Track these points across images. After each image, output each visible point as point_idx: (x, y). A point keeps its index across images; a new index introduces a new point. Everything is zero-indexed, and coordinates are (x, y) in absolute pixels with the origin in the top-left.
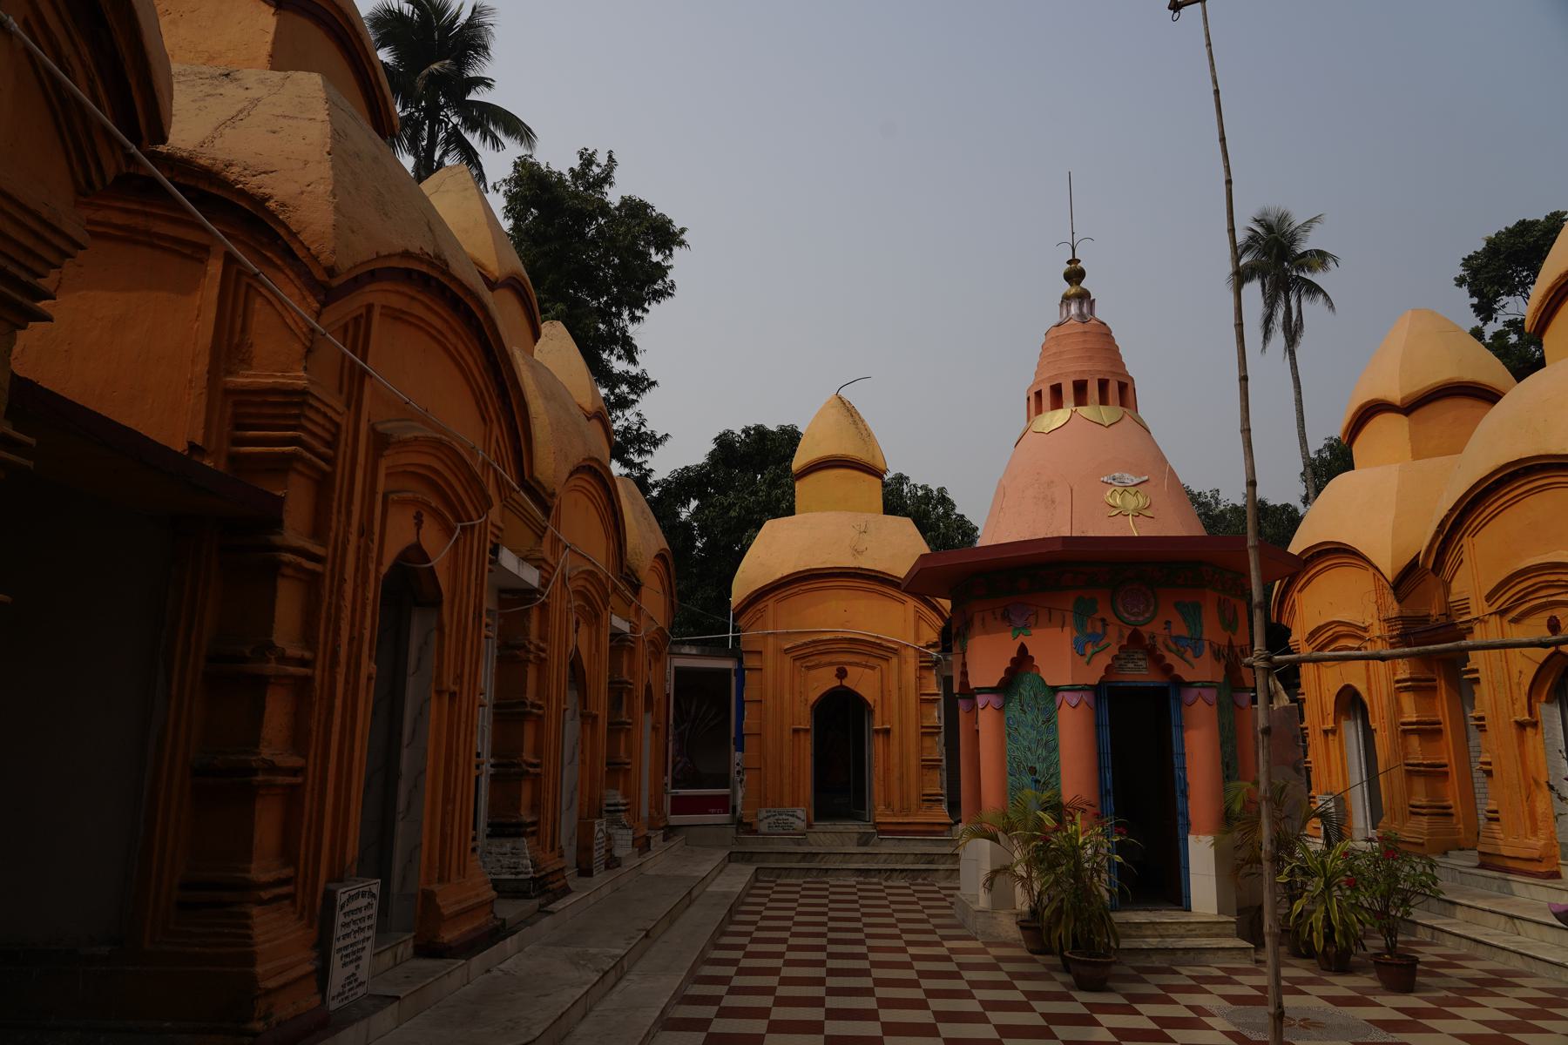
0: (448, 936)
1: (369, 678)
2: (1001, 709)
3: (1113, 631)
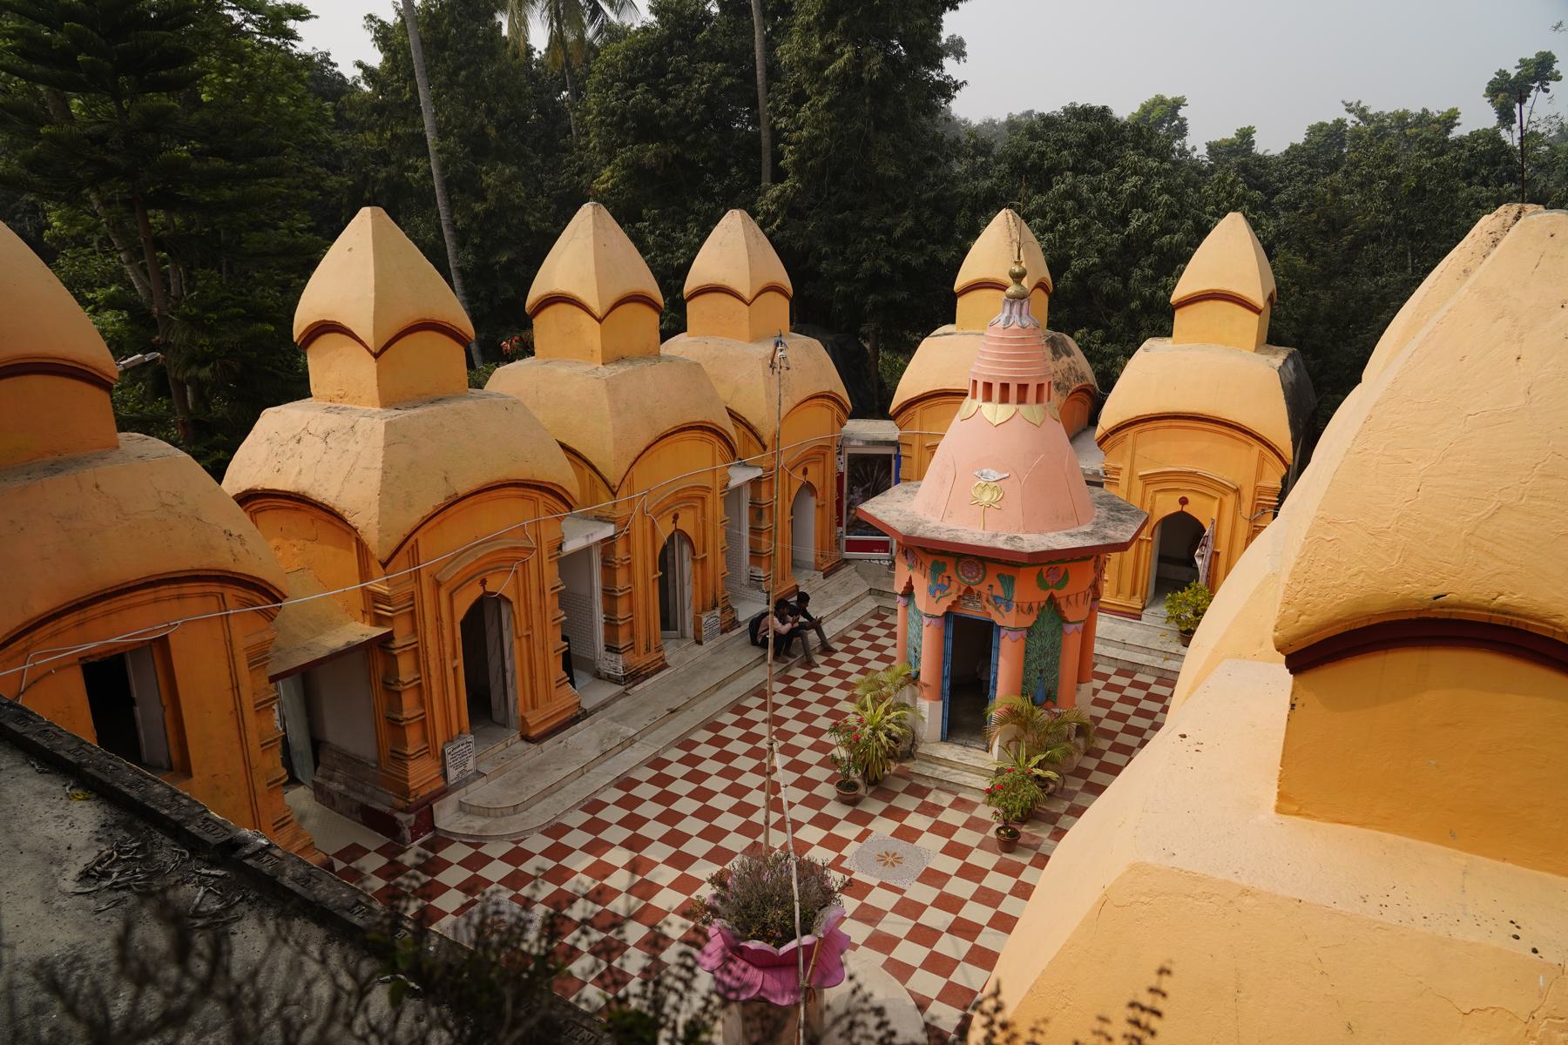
0: (533, 733)
1: (455, 669)
2: (906, 606)
3: (954, 586)
